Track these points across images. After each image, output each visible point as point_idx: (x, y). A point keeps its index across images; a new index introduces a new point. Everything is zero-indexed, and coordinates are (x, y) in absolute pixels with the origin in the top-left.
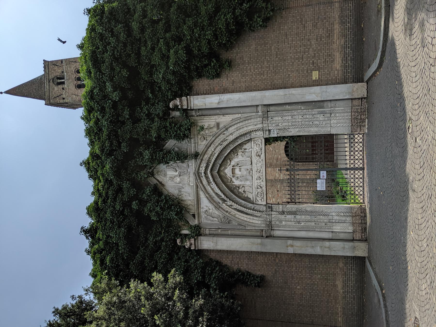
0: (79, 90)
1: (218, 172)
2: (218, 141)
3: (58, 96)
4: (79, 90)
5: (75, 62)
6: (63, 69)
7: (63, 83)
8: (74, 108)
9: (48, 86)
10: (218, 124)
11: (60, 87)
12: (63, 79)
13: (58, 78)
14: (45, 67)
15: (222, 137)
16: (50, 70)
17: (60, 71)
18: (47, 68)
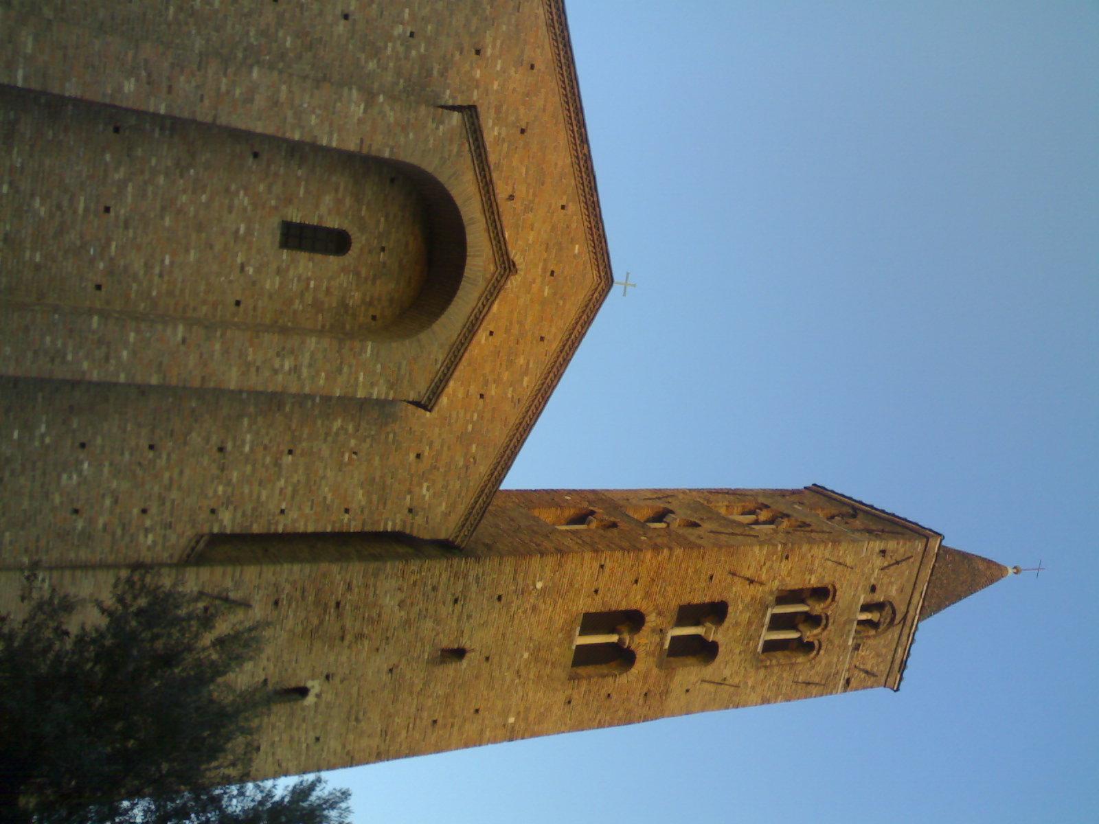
0: (827, 580)
3: (897, 563)
5: (808, 684)
6: (852, 658)
8: (817, 490)
9: (914, 601)
11: (879, 597)
12: (860, 623)
14: (903, 666)
16: (889, 658)
17: (862, 653)
18: (898, 662)
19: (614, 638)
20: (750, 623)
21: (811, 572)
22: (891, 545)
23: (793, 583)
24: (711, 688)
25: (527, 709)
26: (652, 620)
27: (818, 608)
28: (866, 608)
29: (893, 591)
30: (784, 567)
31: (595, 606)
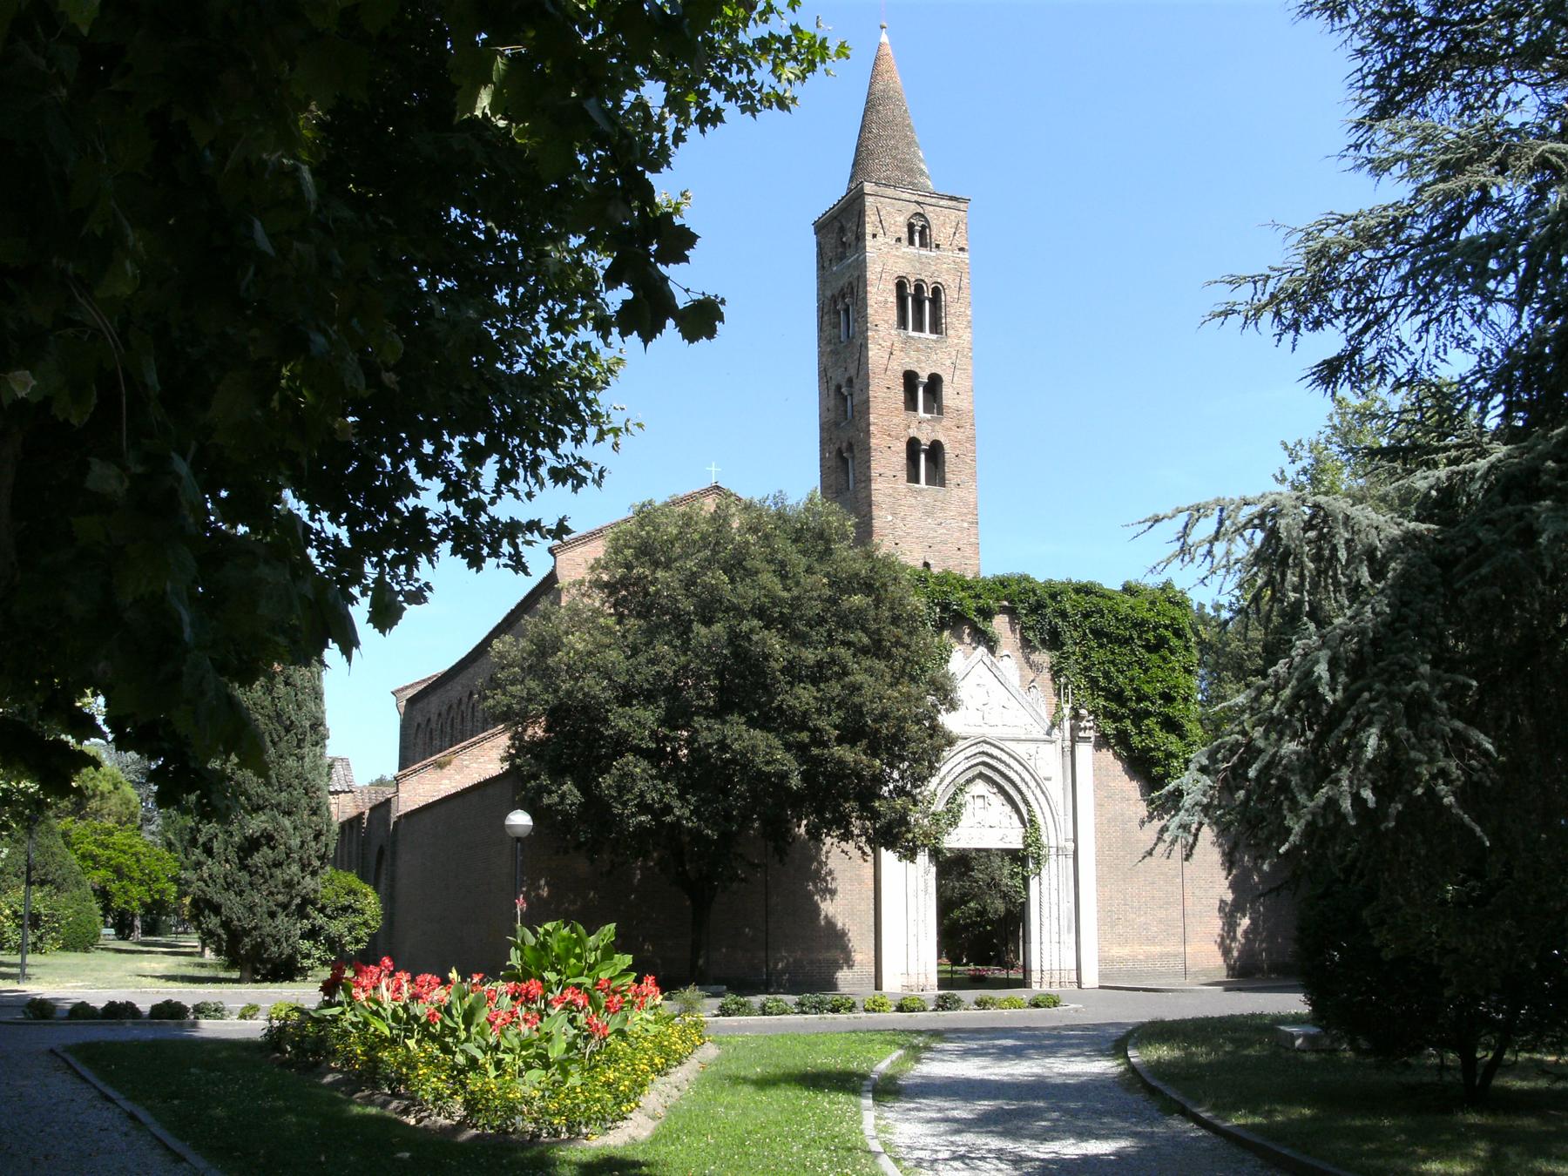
1: (981, 775)
2: (1027, 777)
4: (893, 288)
7: (911, 242)
9: (905, 196)
10: (1048, 779)
13: (923, 227)
15: (1032, 784)
19: (923, 456)
20: (918, 350)
21: (886, 302)
22: (869, 229)
23: (893, 315)
24: (958, 372)
25: (960, 514)
26: (913, 432)
27: (911, 290)
28: (911, 242)
29: (902, 220)
30: (883, 327)
31: (903, 475)
